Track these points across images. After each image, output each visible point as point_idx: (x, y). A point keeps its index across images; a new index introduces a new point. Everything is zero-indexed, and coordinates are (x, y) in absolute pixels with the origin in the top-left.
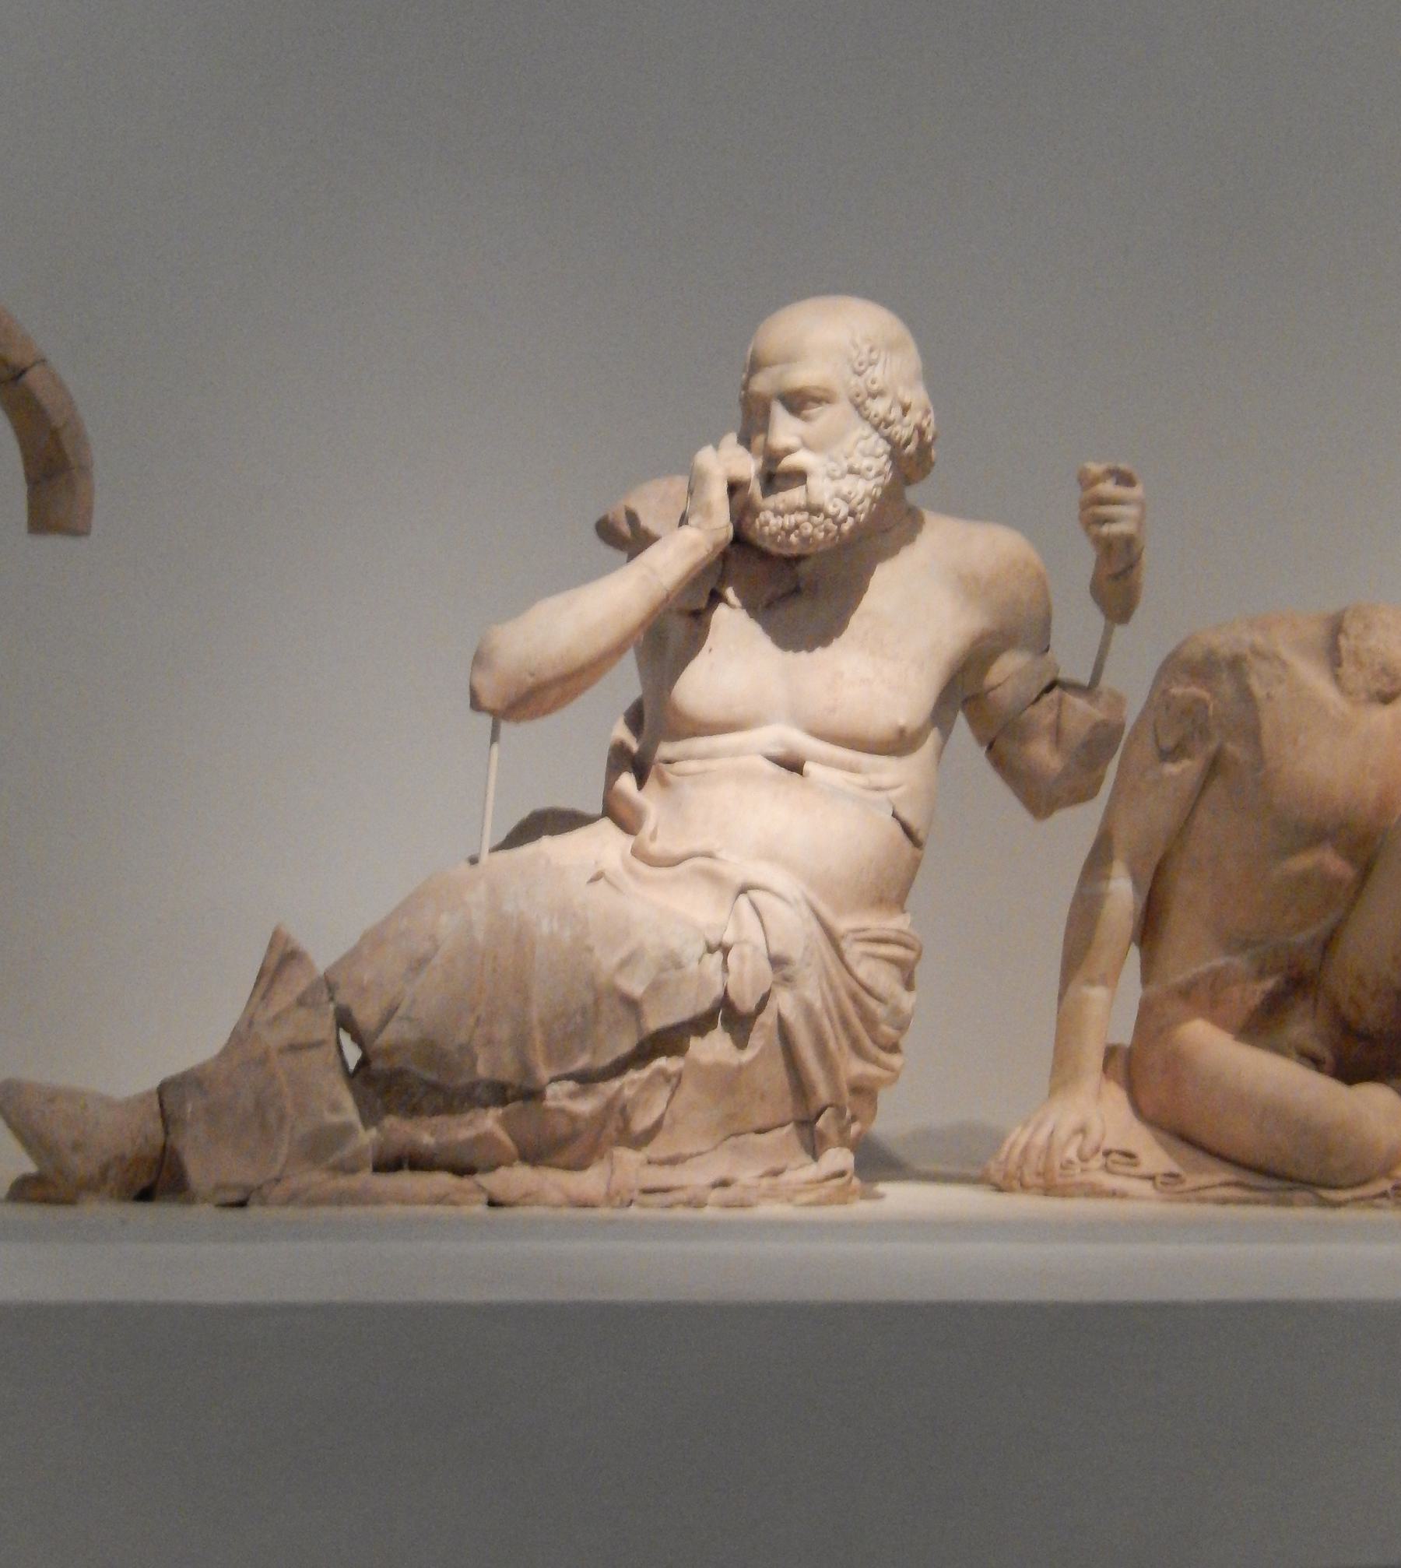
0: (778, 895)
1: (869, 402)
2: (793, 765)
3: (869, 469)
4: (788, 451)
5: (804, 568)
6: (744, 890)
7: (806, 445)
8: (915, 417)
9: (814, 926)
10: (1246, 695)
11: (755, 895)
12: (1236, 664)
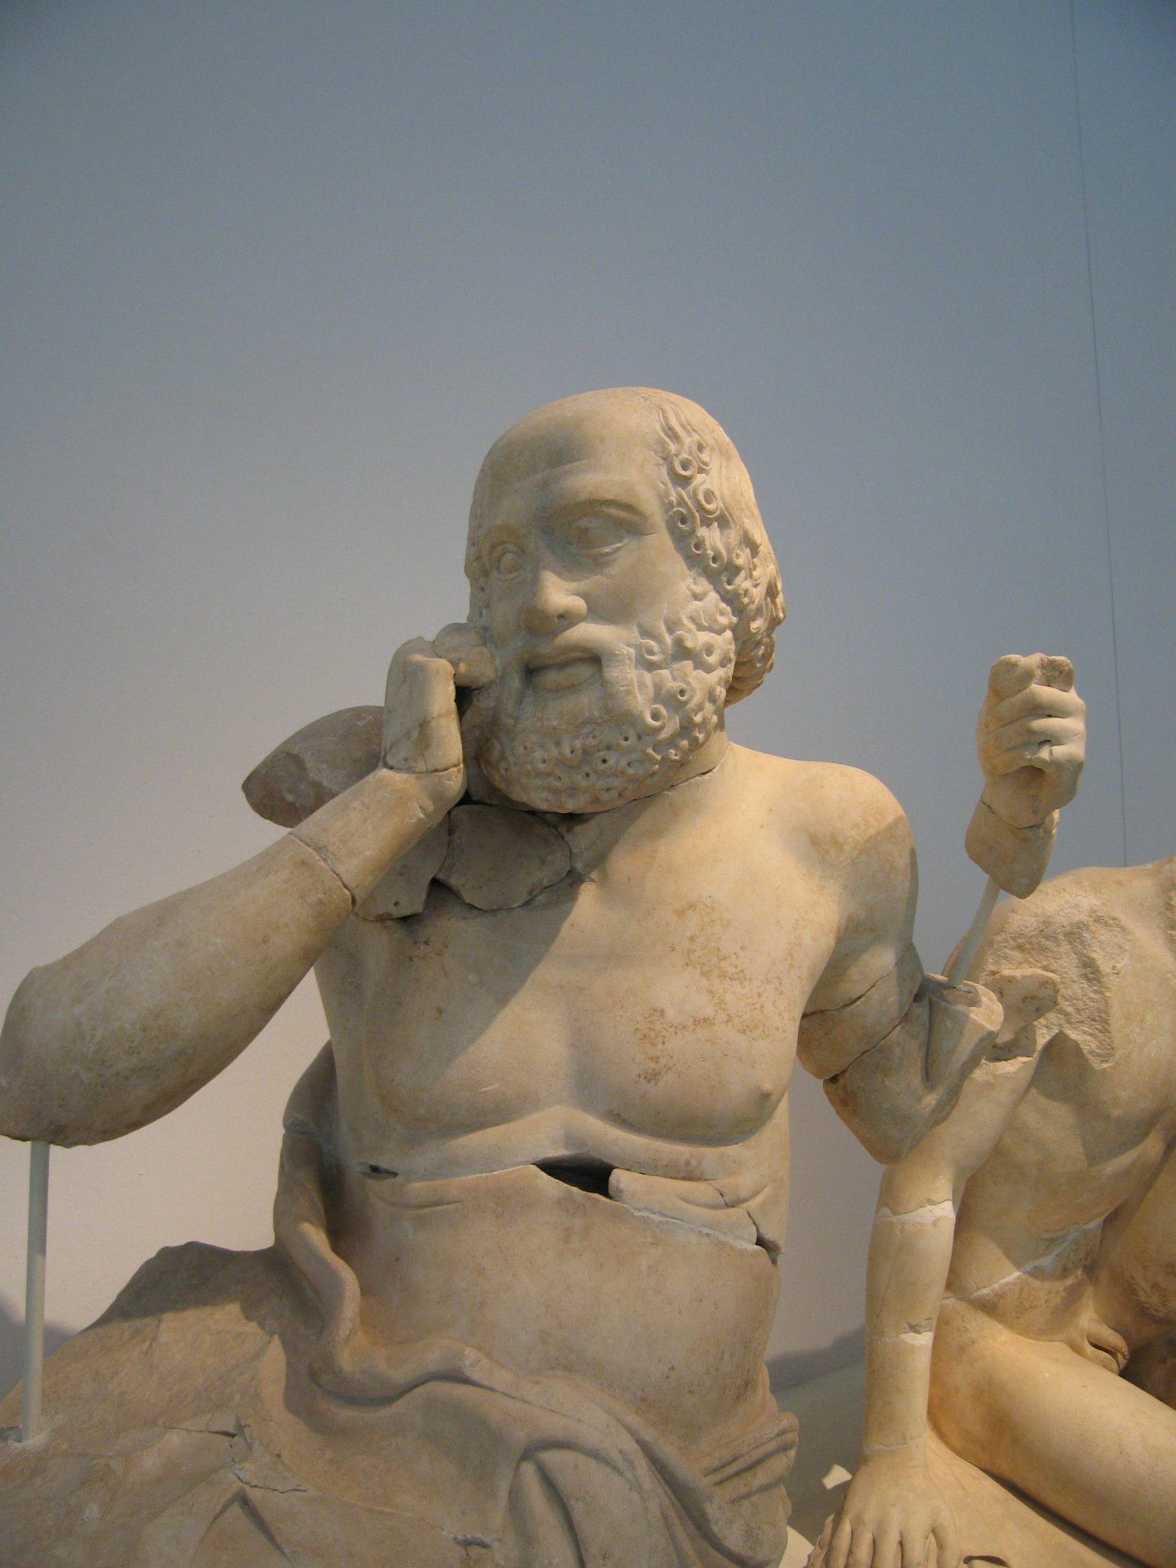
0: (596, 1455)
1: (702, 532)
2: (588, 1174)
3: (709, 650)
4: (567, 618)
5: (583, 837)
6: (529, 1453)
7: (597, 612)
8: (767, 570)
9: (657, 1497)
10: (1091, 971)
11: (549, 1457)
12: (1074, 934)
